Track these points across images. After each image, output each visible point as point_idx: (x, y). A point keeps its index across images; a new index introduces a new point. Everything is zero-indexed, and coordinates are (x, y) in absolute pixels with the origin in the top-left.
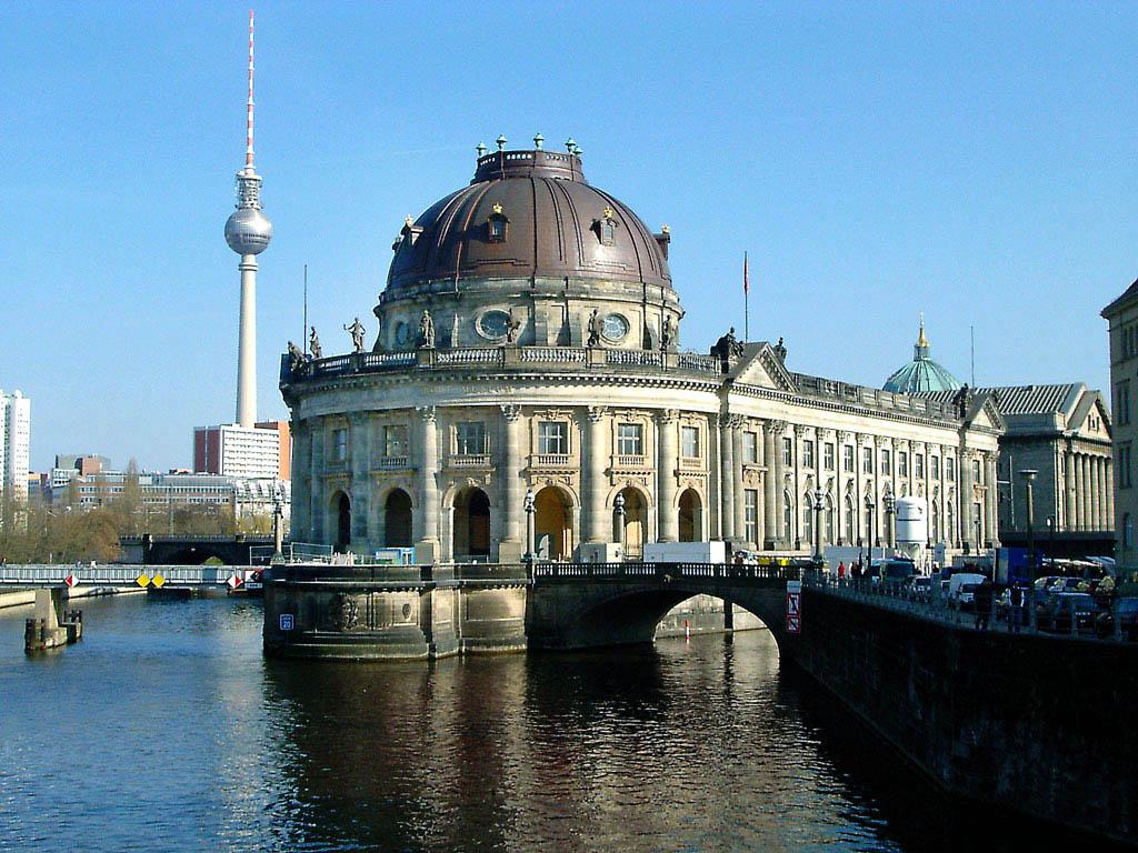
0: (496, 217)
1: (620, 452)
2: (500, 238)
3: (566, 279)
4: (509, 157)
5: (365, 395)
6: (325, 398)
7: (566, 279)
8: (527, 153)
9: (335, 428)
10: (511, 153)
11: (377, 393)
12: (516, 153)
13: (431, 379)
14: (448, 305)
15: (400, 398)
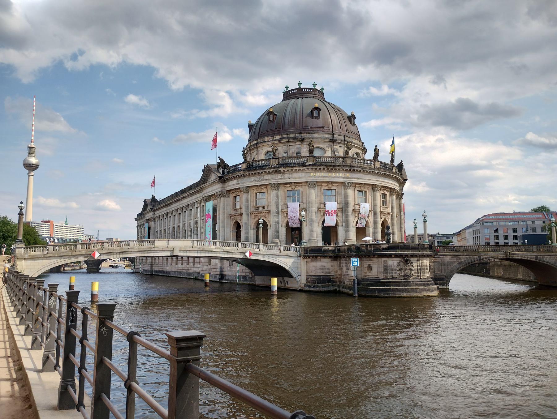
0: (316, 108)
1: (383, 205)
2: (318, 117)
3: (344, 136)
4: (303, 90)
5: (279, 176)
6: (253, 178)
7: (344, 136)
8: (311, 89)
9: (235, 195)
10: (304, 89)
11: (287, 175)
12: (307, 89)
13: (316, 169)
14: (297, 143)
15: (299, 178)
